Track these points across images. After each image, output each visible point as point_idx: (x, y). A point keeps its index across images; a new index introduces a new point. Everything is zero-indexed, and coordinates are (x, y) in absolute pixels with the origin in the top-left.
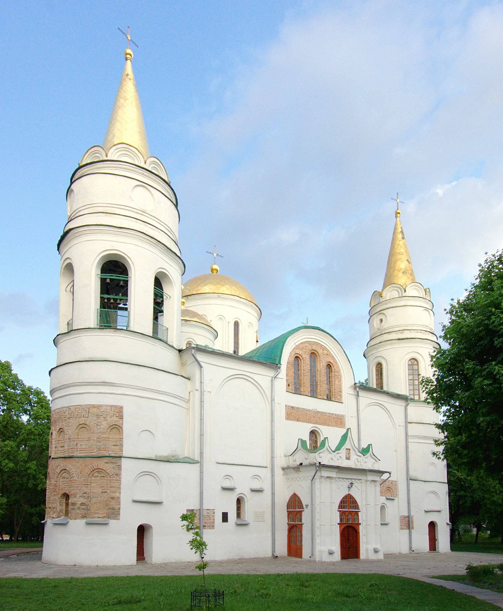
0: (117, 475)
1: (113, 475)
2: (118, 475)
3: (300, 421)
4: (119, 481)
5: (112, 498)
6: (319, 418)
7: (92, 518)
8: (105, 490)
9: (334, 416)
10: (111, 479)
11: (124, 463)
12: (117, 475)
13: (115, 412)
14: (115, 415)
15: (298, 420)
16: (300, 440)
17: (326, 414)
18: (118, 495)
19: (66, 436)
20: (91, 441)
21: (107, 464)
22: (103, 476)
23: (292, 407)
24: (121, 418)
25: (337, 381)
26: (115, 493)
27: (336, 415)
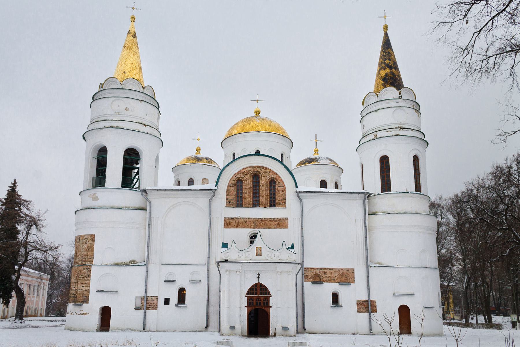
0: (89, 276)
1: (87, 276)
2: (89, 276)
3: (240, 227)
4: (89, 280)
5: (85, 290)
6: (260, 223)
7: (78, 302)
10: (86, 278)
11: (93, 268)
12: (89, 276)
13: (90, 238)
14: (91, 240)
15: (237, 227)
17: (267, 219)
18: (88, 289)
21: (84, 270)
23: (231, 218)
24: (93, 241)
25: (281, 192)
26: (87, 287)
27: (278, 219)
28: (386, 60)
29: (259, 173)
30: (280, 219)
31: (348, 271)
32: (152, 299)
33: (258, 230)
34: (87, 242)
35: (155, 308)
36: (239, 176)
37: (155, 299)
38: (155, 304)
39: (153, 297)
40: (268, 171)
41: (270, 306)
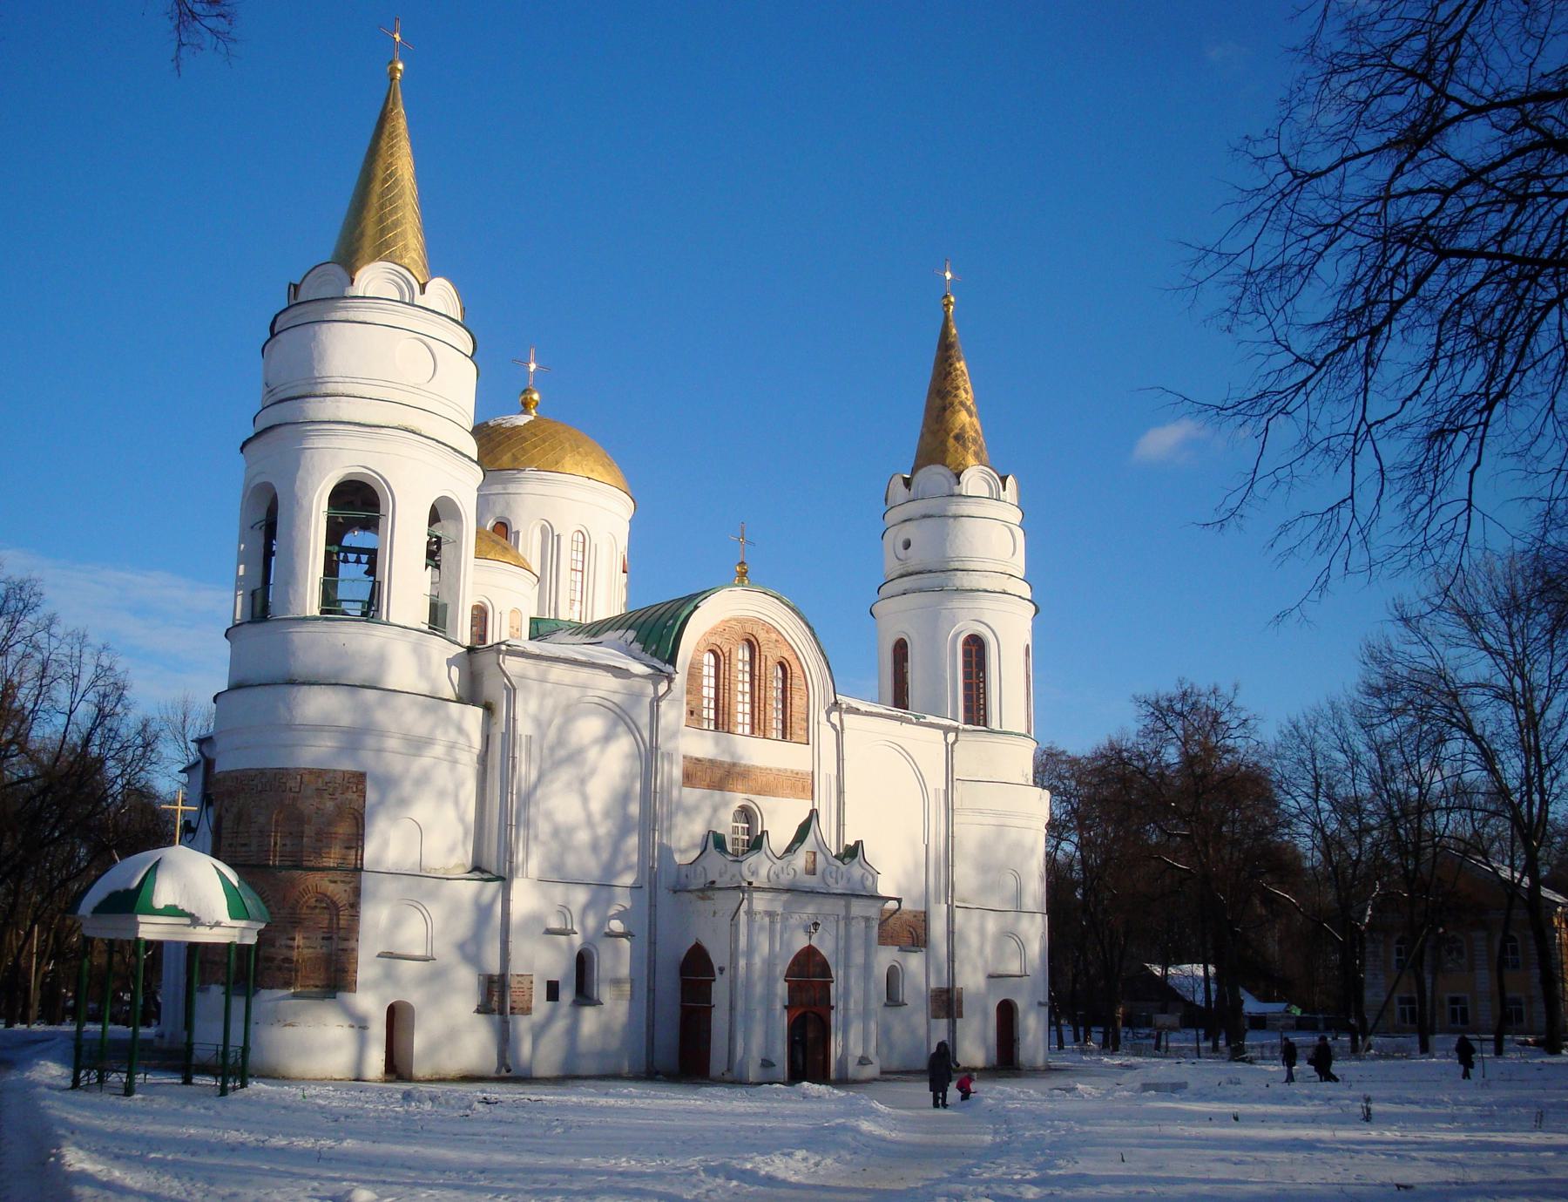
8: (329, 935)
9: (789, 774)
16: (711, 833)
19: (253, 825)
20: (305, 839)
21: (333, 885)
22: (325, 908)
27: (792, 772)
28: (957, 388)
29: (753, 639)
30: (797, 774)
31: (915, 916)
32: (519, 982)
33: (752, 797)
34: (337, 795)
35: (527, 1011)
36: (713, 640)
37: (526, 985)
38: (526, 998)
39: (522, 975)
40: (774, 636)
41: (833, 1003)
